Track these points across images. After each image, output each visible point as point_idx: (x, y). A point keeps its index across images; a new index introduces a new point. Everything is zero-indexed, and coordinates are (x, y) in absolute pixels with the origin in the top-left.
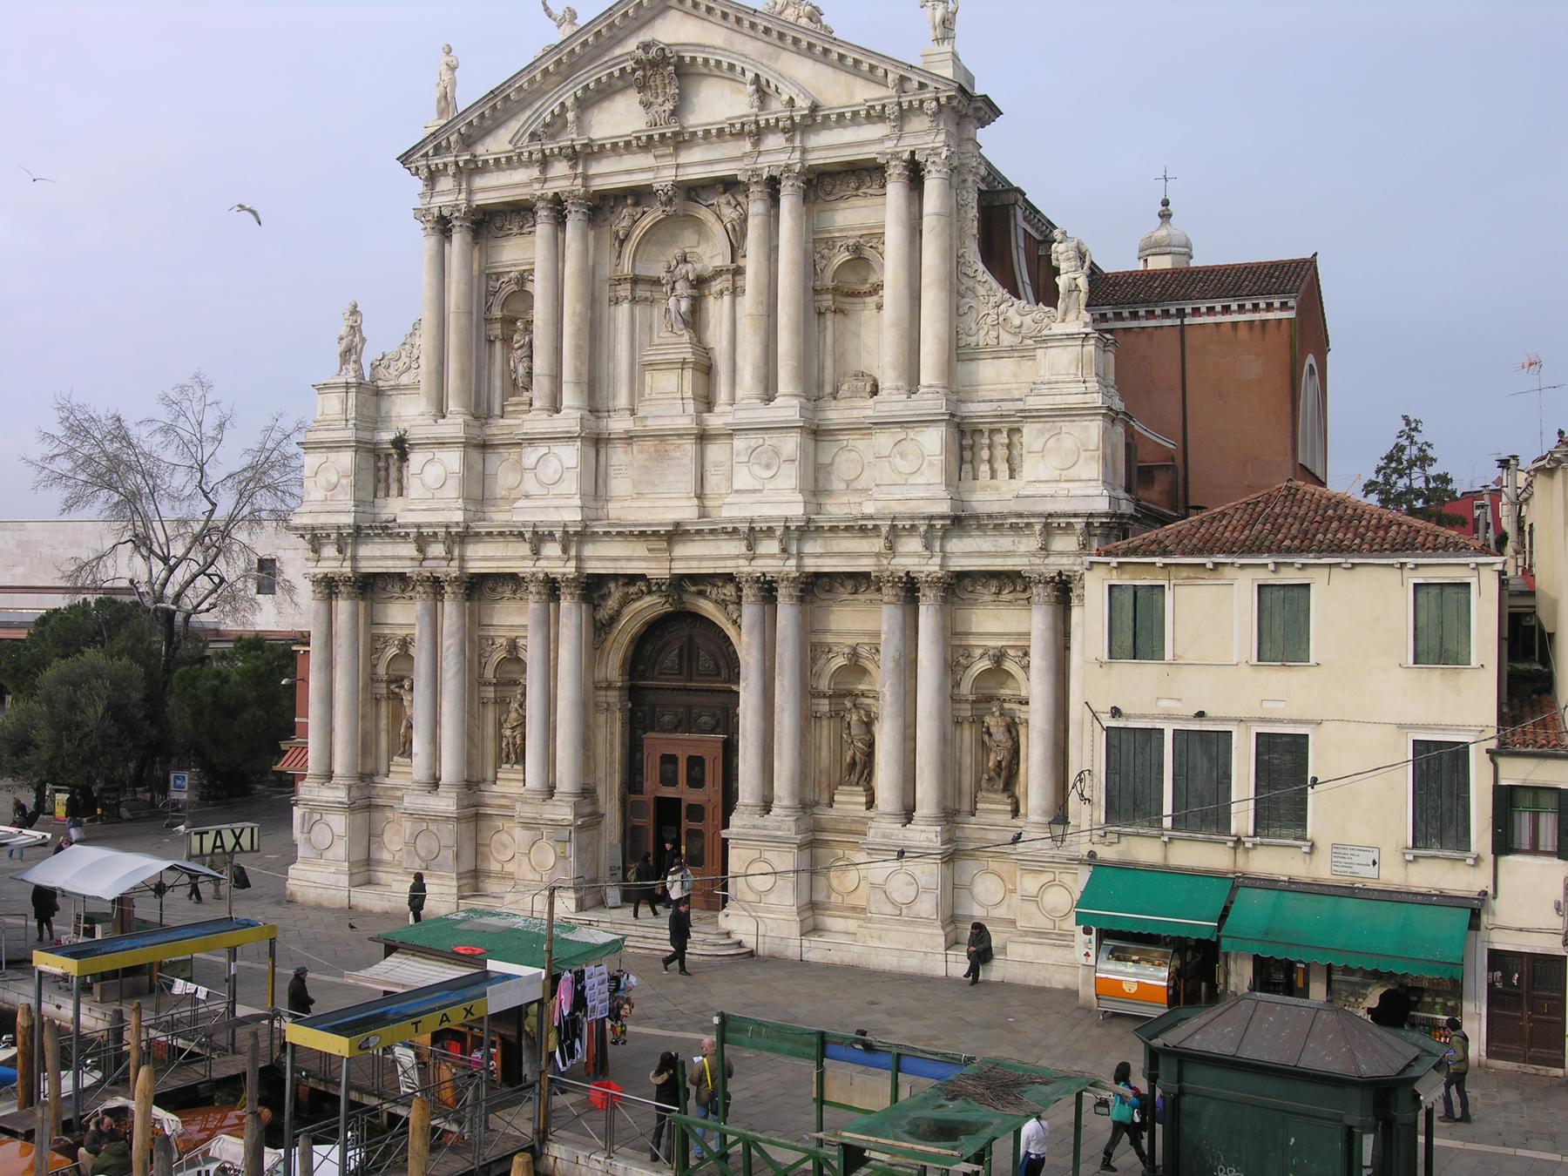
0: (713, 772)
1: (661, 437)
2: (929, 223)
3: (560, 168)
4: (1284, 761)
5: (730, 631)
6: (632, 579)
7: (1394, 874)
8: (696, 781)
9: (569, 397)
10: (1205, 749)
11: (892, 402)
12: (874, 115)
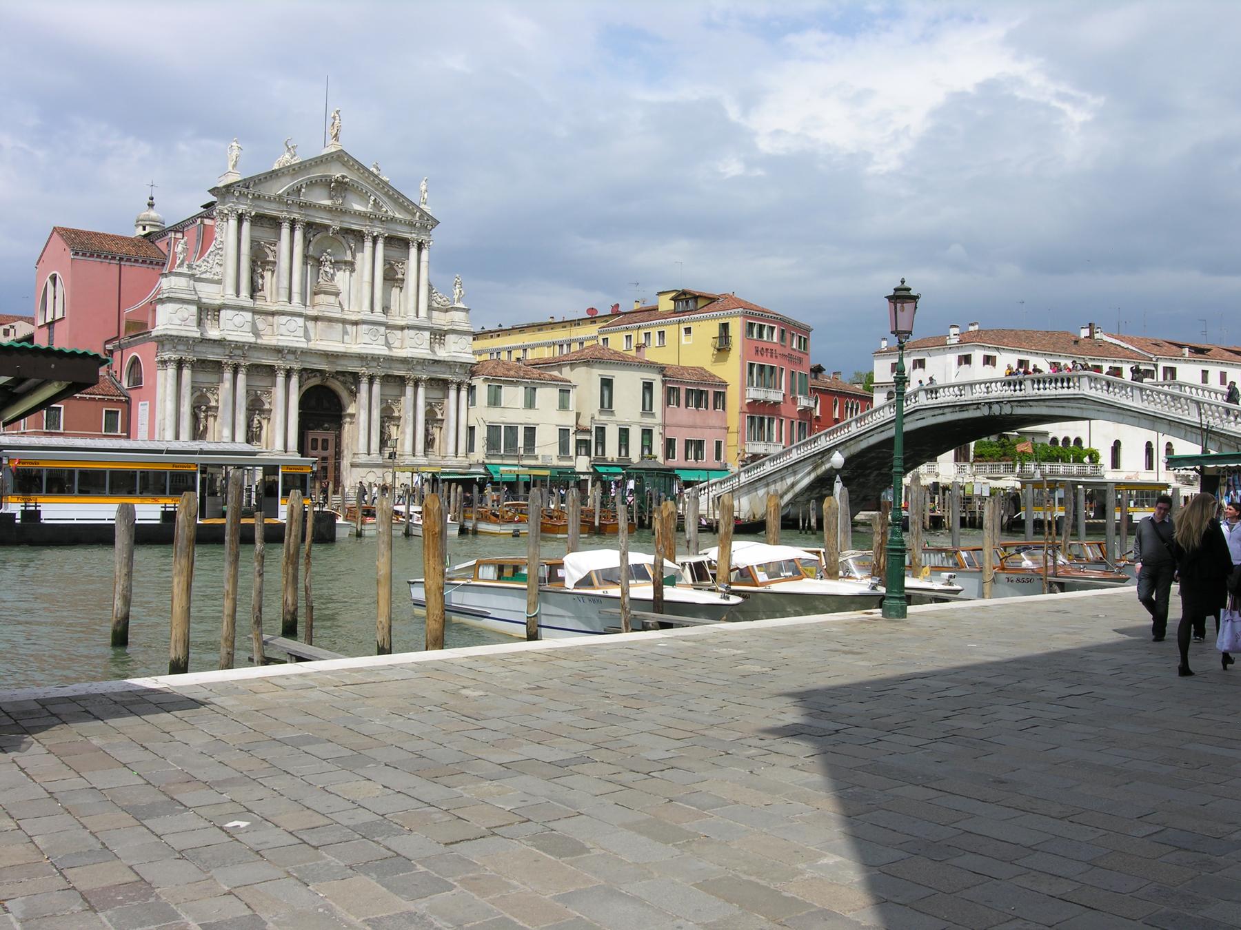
0: (332, 445)
1: (330, 320)
2: (424, 265)
3: (295, 209)
4: (530, 432)
5: (344, 394)
6: (313, 371)
7: (556, 462)
8: (325, 448)
9: (296, 298)
10: (512, 429)
11: (413, 321)
12: (411, 225)
